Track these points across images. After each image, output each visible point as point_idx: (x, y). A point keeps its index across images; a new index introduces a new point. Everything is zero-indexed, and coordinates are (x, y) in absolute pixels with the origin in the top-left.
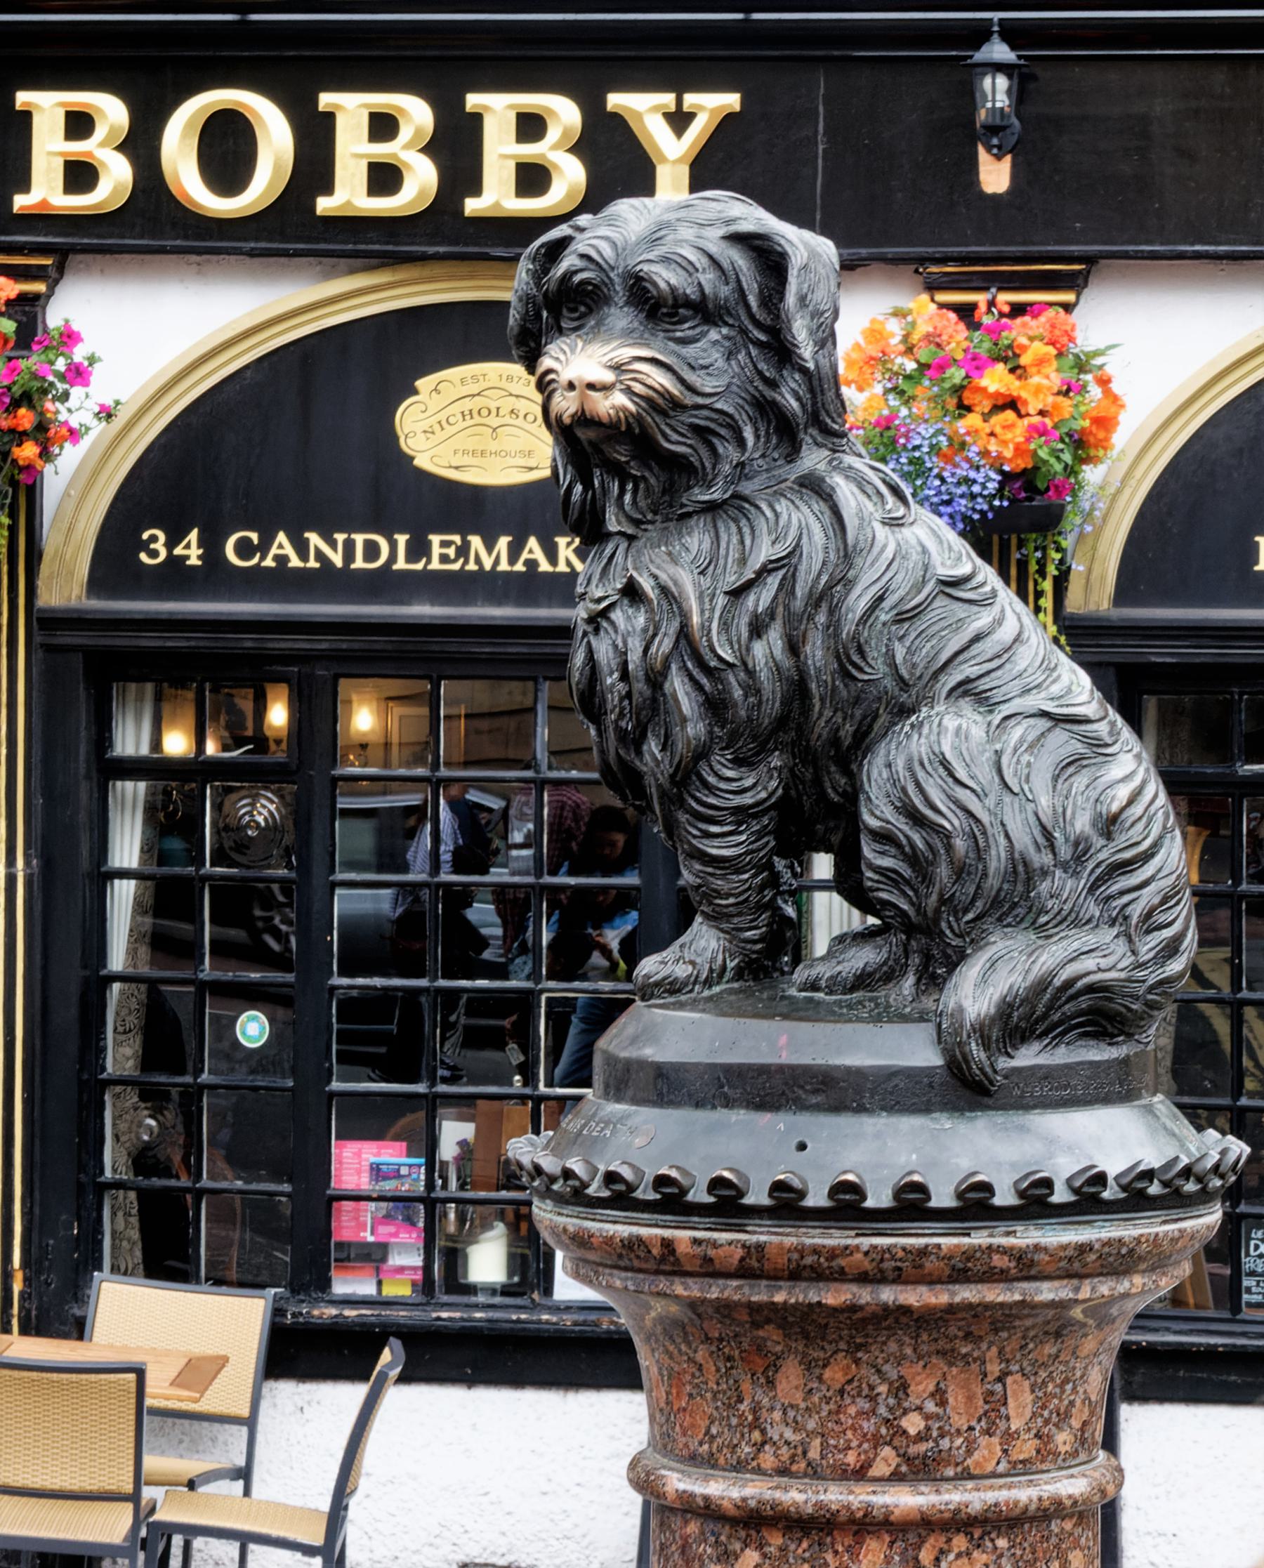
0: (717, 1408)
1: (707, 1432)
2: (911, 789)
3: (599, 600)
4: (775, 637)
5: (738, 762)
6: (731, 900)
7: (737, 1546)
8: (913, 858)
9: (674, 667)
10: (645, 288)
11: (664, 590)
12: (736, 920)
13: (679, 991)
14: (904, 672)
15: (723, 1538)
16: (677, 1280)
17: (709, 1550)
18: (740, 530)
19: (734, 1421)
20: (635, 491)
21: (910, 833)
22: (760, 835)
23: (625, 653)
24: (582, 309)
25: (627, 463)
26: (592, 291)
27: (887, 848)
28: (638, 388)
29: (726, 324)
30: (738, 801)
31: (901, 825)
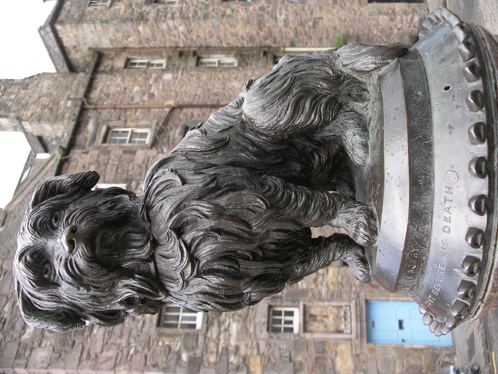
2: (273, 95)
3: (182, 252)
4: (205, 171)
5: (262, 185)
6: (327, 199)
8: (306, 92)
9: (213, 202)
11: (178, 209)
12: (336, 200)
13: (372, 213)
14: (226, 127)
18: (158, 194)
20: (135, 240)
21: (294, 94)
22: (296, 187)
23: (206, 230)
24: (47, 266)
25: (118, 234)
26: (38, 257)
27: (301, 106)
28: (80, 218)
29: (70, 203)
30: (280, 186)
31: (291, 99)
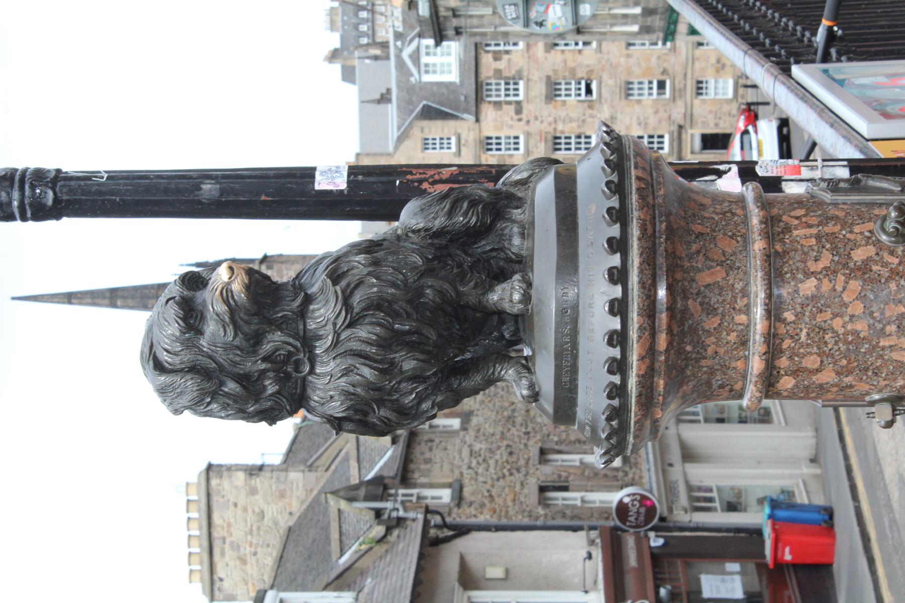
0: (719, 231)
1: (731, 237)
7: (781, 224)
10: (188, 280)
15: (780, 230)
16: (656, 194)
17: (787, 237)
19: (724, 223)
